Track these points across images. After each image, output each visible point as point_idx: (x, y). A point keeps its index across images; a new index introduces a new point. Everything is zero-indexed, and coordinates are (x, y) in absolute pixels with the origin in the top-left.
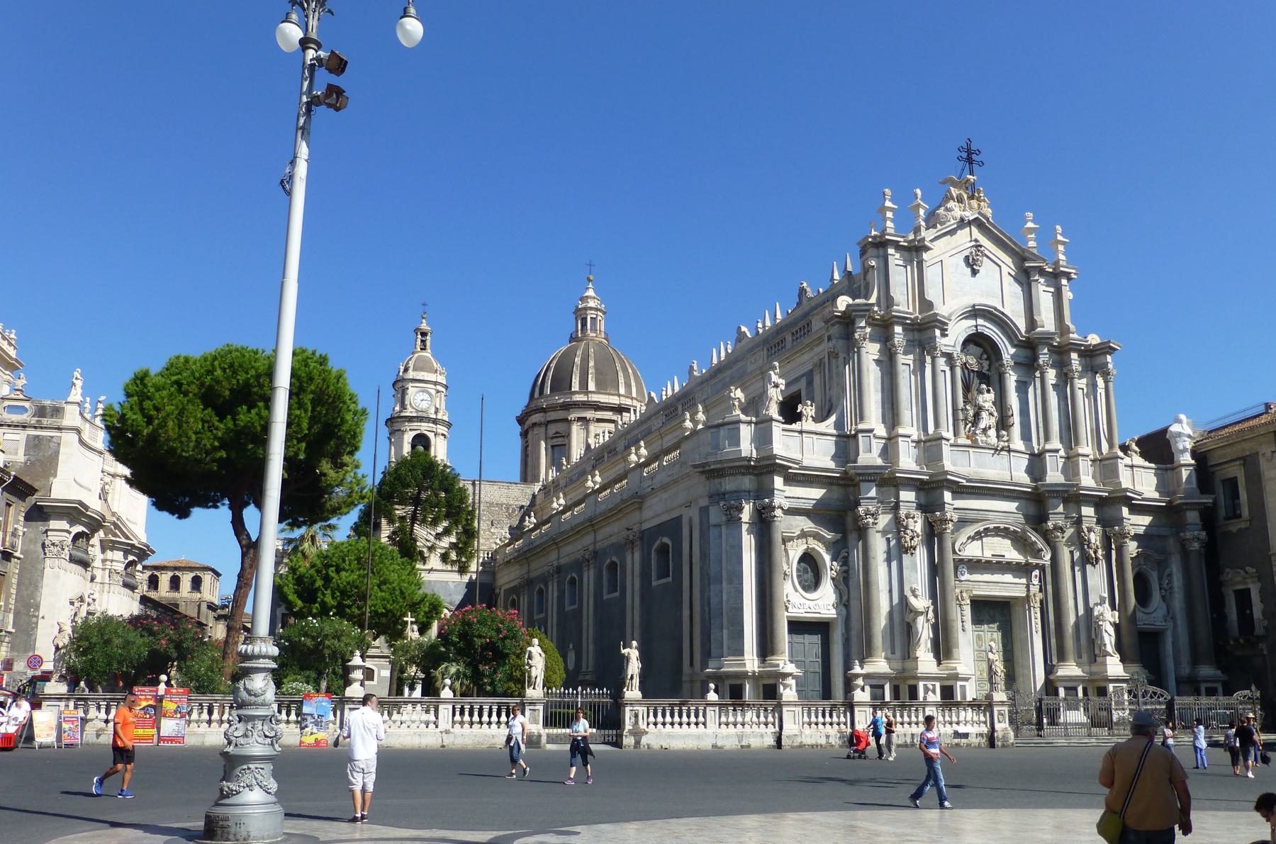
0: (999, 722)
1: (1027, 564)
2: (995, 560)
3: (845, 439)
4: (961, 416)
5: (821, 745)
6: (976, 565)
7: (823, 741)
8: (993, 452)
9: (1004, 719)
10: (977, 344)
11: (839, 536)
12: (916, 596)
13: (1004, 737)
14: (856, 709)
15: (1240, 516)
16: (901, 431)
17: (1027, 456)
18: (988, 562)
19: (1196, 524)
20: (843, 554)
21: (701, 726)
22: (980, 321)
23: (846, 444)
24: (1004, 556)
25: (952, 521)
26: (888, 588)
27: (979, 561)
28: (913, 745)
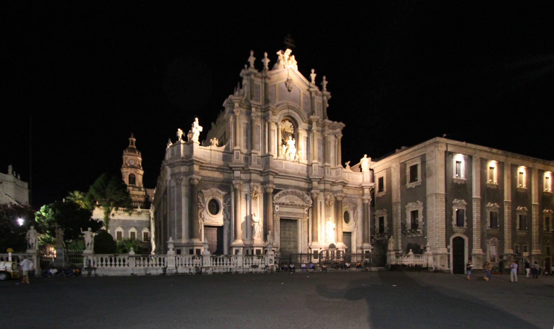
0: (270, 263)
1: (303, 206)
2: (290, 204)
3: (231, 155)
5: (186, 273)
7: (188, 271)
8: (292, 163)
9: (272, 262)
11: (227, 193)
12: (255, 216)
13: (271, 269)
14: (204, 258)
15: (383, 191)
16: (253, 151)
17: (306, 166)
18: (287, 204)
19: (367, 194)
20: (229, 200)
23: (228, 155)
24: (294, 203)
25: (273, 188)
26: (246, 214)
27: (283, 204)
28: (230, 272)
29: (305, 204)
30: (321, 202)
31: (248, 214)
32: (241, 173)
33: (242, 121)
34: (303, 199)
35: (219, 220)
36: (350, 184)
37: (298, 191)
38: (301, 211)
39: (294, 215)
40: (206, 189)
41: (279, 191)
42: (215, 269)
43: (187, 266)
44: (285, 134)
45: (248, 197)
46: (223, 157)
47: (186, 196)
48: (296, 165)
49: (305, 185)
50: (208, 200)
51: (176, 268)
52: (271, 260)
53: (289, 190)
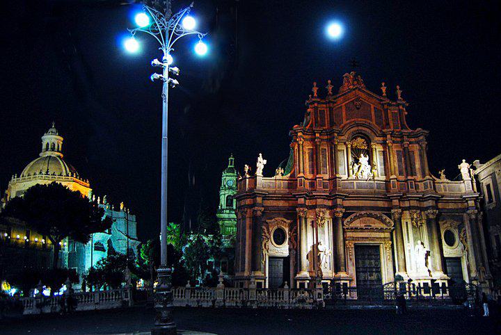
0: (319, 298)
4: (351, 167)
6: (355, 229)
10: (362, 138)
14: (250, 292)
20: (295, 228)
21: (183, 298)
22: (360, 128)
27: (356, 228)
29: (384, 226)
30: (407, 223)
31: (315, 243)
32: (305, 199)
33: (308, 147)
34: (383, 221)
35: (284, 250)
36: (446, 197)
37: (373, 212)
38: (382, 235)
39: (372, 240)
40: (271, 219)
41: (350, 214)
42: (261, 303)
43: (235, 299)
44: (356, 153)
45: (314, 224)
46: (288, 185)
47: (250, 228)
48: (371, 183)
49: (384, 204)
50: (272, 230)
51: (224, 301)
52: (319, 294)
53: (363, 213)
